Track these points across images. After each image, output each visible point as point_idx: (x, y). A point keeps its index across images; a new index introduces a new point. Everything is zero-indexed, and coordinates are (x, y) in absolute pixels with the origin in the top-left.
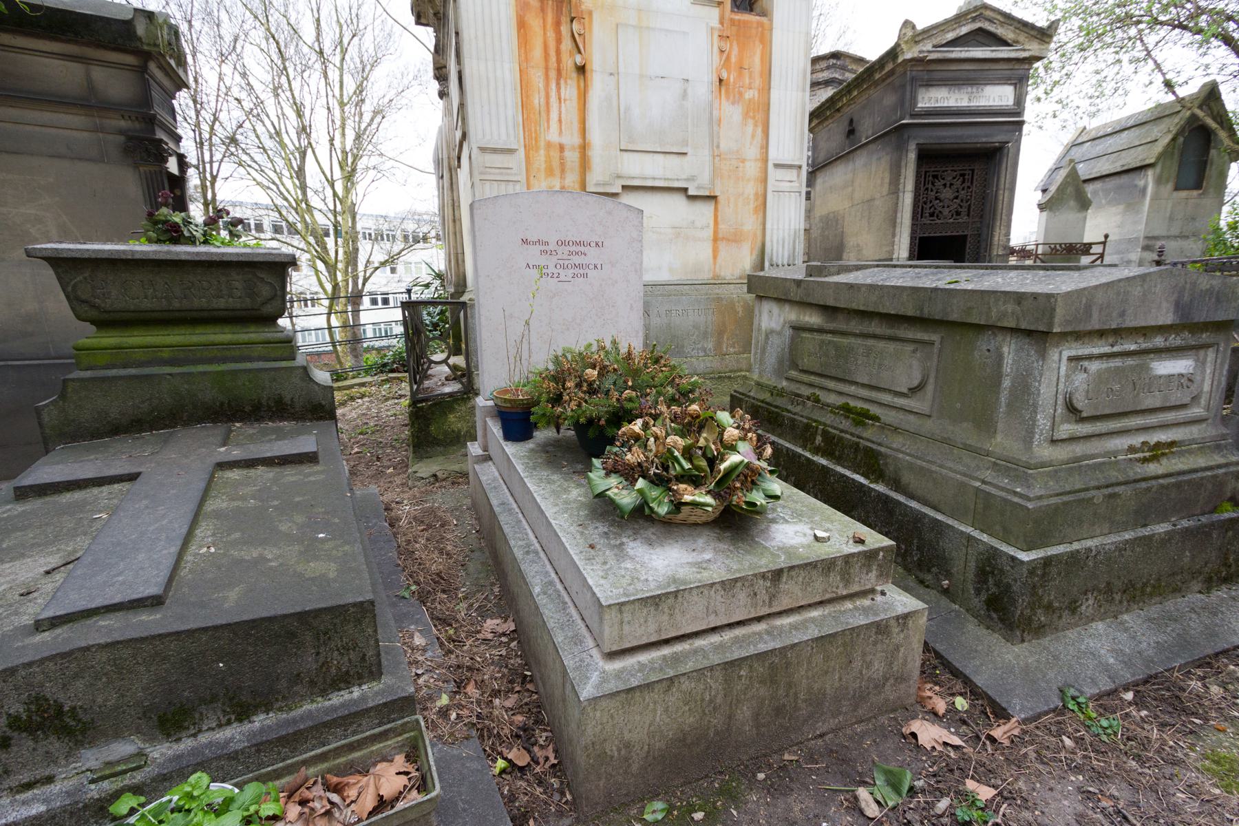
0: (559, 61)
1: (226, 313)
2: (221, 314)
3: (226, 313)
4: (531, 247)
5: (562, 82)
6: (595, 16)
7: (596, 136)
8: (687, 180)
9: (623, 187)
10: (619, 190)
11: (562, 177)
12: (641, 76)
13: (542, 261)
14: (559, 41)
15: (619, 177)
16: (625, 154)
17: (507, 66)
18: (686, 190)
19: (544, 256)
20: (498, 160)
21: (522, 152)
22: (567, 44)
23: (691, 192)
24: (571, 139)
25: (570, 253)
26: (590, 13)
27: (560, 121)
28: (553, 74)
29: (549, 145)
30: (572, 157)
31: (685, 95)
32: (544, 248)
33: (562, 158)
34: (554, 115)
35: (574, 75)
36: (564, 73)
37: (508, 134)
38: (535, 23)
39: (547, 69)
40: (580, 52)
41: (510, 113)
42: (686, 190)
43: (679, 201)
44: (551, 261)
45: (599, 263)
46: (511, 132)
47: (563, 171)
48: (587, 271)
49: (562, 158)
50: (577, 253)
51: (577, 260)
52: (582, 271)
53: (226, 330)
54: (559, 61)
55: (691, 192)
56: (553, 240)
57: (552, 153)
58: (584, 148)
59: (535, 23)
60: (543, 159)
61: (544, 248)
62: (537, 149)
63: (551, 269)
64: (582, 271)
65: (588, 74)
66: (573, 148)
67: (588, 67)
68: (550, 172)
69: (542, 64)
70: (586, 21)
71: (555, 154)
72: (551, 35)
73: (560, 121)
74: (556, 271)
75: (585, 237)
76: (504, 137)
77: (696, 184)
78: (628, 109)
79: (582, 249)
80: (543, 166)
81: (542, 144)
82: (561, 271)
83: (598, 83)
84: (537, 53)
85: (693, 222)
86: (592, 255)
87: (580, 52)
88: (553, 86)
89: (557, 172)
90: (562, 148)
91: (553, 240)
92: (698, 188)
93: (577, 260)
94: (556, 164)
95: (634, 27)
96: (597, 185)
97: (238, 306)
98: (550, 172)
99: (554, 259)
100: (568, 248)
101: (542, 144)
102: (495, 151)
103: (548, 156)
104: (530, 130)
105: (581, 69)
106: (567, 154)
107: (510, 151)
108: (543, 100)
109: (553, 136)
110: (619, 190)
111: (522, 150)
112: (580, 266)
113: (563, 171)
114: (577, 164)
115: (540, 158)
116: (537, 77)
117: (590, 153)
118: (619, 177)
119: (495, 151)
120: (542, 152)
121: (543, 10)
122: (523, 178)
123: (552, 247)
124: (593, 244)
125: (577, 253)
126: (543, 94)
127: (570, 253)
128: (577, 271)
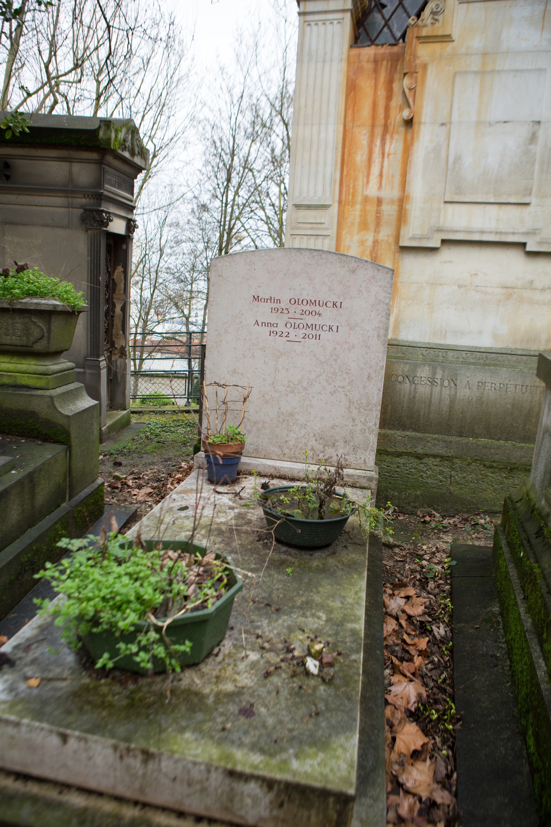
0: (387, 116)
1: (12, 347)
2: (8, 348)
3: (12, 347)
4: (261, 304)
5: (388, 137)
6: (430, 69)
7: (417, 188)
8: (527, 234)
9: (444, 242)
10: (438, 244)
11: (377, 230)
12: (479, 123)
13: (272, 318)
14: (389, 97)
15: (439, 230)
16: (450, 207)
17: (331, 128)
18: (524, 245)
19: (274, 315)
20: (311, 216)
21: (335, 209)
22: (397, 100)
23: (529, 248)
24: (390, 192)
25: (303, 313)
26: (425, 67)
27: (381, 175)
28: (379, 131)
29: (366, 199)
30: (389, 211)
31: (533, 138)
32: (275, 305)
33: (378, 212)
34: (375, 170)
35: (402, 129)
36: (391, 129)
37: (324, 192)
38: (366, 85)
39: (373, 126)
40: (409, 107)
41: (329, 170)
42: (524, 245)
43: (514, 260)
44: (281, 320)
45: (335, 324)
46: (328, 189)
47: (378, 224)
48: (320, 332)
49: (378, 212)
50: (310, 313)
51: (310, 320)
52: (314, 332)
53: (23, 362)
54: (387, 116)
55: (529, 248)
56: (285, 297)
57: (368, 208)
58: (402, 202)
59: (366, 85)
60: (358, 213)
61: (275, 305)
62: (353, 204)
63: (281, 328)
64: (314, 332)
65: (416, 126)
66: (392, 202)
67: (415, 120)
68: (364, 226)
69: (369, 122)
70: (419, 75)
71: (372, 208)
72: (382, 93)
73: (381, 175)
74: (285, 330)
75: (322, 297)
76: (319, 194)
77: (538, 238)
78: (458, 159)
79: (317, 309)
80: (358, 220)
81: (359, 198)
82: (291, 330)
83: (426, 136)
84: (365, 111)
85: (532, 282)
86: (328, 316)
87: (409, 107)
88: (378, 142)
89: (372, 226)
90: (379, 201)
91: (285, 297)
92: (540, 243)
93: (310, 320)
94: (371, 218)
95: (475, 72)
96: (413, 238)
97: (18, 343)
98: (364, 226)
99: (285, 317)
100: (302, 307)
101: (359, 198)
102: (309, 207)
103: (364, 211)
104: (348, 186)
105: (409, 123)
106: (385, 207)
107: (324, 207)
108: (365, 157)
109: (372, 191)
110: (438, 244)
111: (336, 206)
112: (312, 327)
113: (378, 224)
114: (394, 218)
115: (355, 214)
116: (362, 137)
117: (408, 206)
118: (439, 230)
119: (309, 207)
120: (358, 207)
121: (376, 71)
122: (333, 232)
123: (283, 305)
124: (330, 304)
125: (310, 313)
126: (366, 150)
127: (303, 313)
128: (308, 331)
